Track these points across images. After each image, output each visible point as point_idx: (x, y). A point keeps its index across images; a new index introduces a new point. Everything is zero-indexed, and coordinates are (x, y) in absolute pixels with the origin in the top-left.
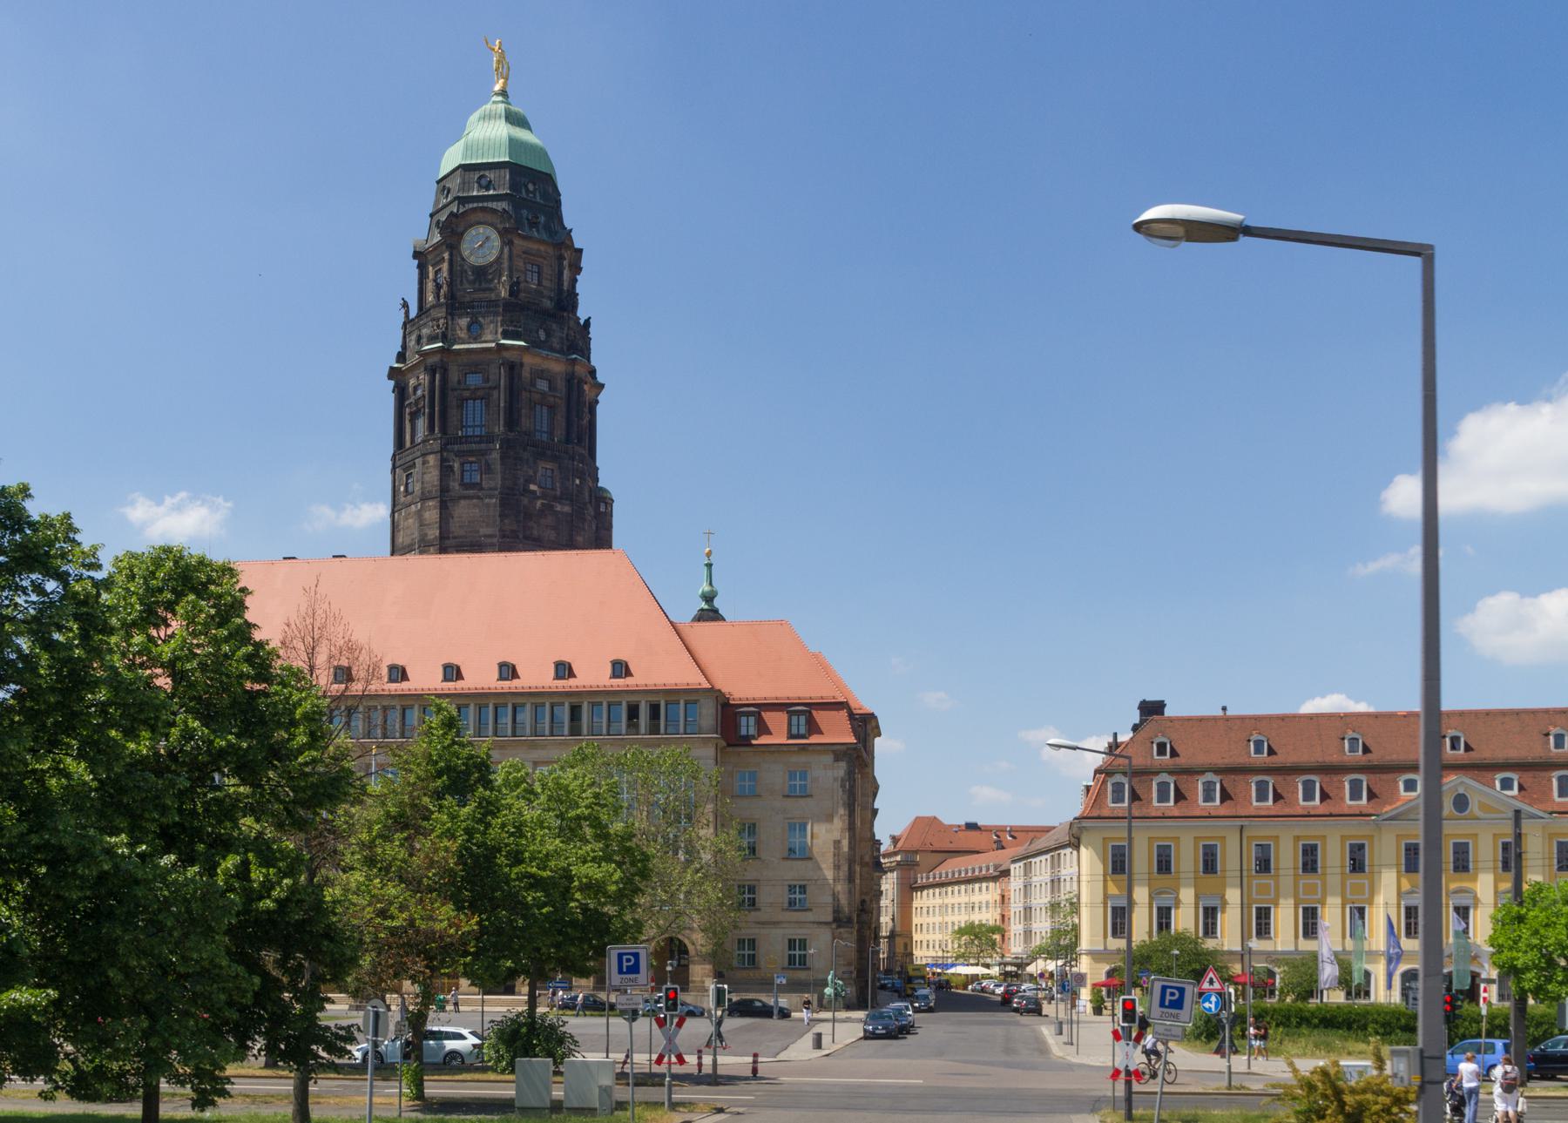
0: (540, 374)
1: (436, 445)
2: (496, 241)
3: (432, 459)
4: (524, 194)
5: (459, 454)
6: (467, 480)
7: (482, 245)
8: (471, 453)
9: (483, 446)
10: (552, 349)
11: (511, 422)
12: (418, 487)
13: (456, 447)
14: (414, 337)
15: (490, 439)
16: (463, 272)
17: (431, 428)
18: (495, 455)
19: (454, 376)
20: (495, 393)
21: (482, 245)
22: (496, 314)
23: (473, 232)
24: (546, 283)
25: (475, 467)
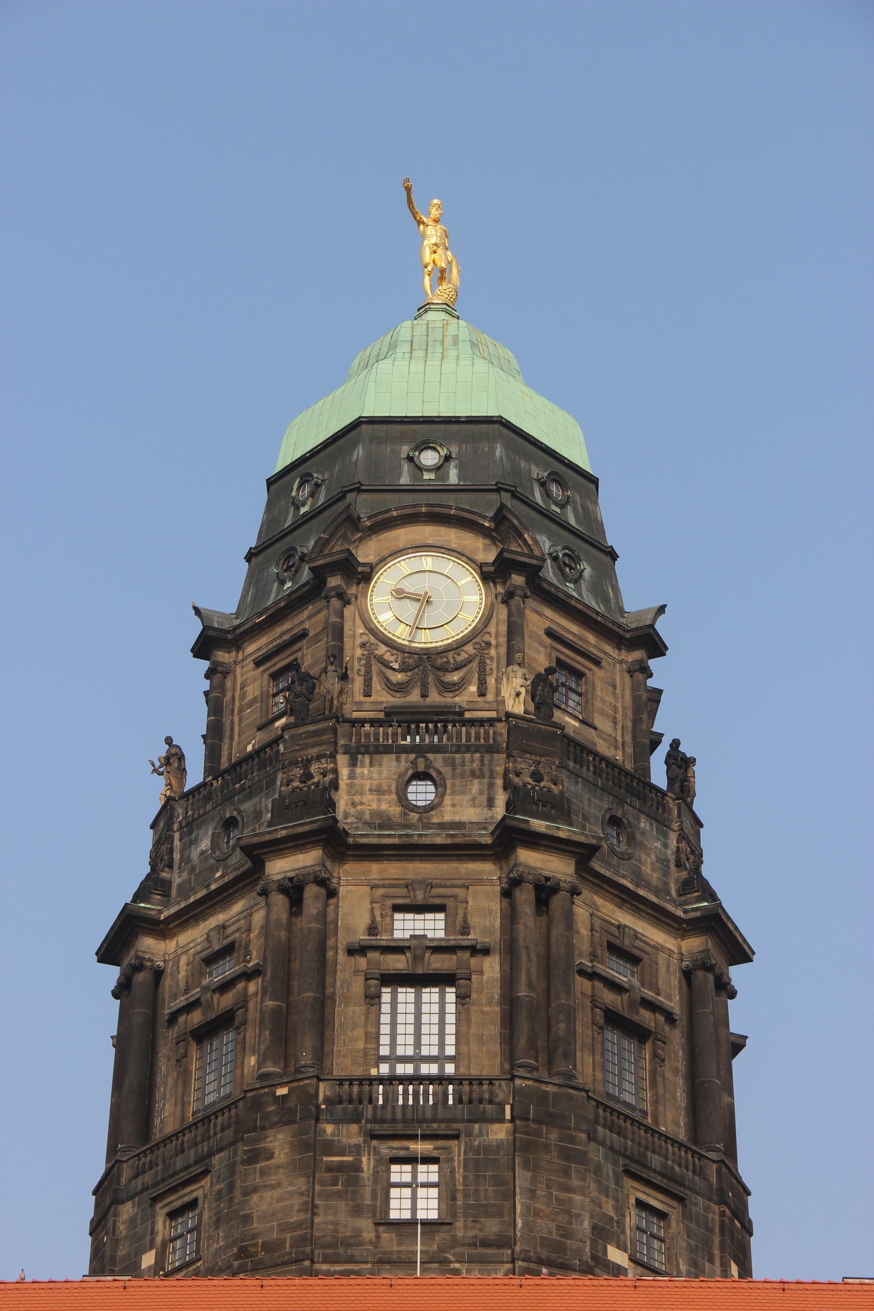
4: (538, 497)
16: (371, 657)
21: (426, 594)
22: (491, 749)
23: (403, 566)
24: (599, 721)
25: (429, 1173)
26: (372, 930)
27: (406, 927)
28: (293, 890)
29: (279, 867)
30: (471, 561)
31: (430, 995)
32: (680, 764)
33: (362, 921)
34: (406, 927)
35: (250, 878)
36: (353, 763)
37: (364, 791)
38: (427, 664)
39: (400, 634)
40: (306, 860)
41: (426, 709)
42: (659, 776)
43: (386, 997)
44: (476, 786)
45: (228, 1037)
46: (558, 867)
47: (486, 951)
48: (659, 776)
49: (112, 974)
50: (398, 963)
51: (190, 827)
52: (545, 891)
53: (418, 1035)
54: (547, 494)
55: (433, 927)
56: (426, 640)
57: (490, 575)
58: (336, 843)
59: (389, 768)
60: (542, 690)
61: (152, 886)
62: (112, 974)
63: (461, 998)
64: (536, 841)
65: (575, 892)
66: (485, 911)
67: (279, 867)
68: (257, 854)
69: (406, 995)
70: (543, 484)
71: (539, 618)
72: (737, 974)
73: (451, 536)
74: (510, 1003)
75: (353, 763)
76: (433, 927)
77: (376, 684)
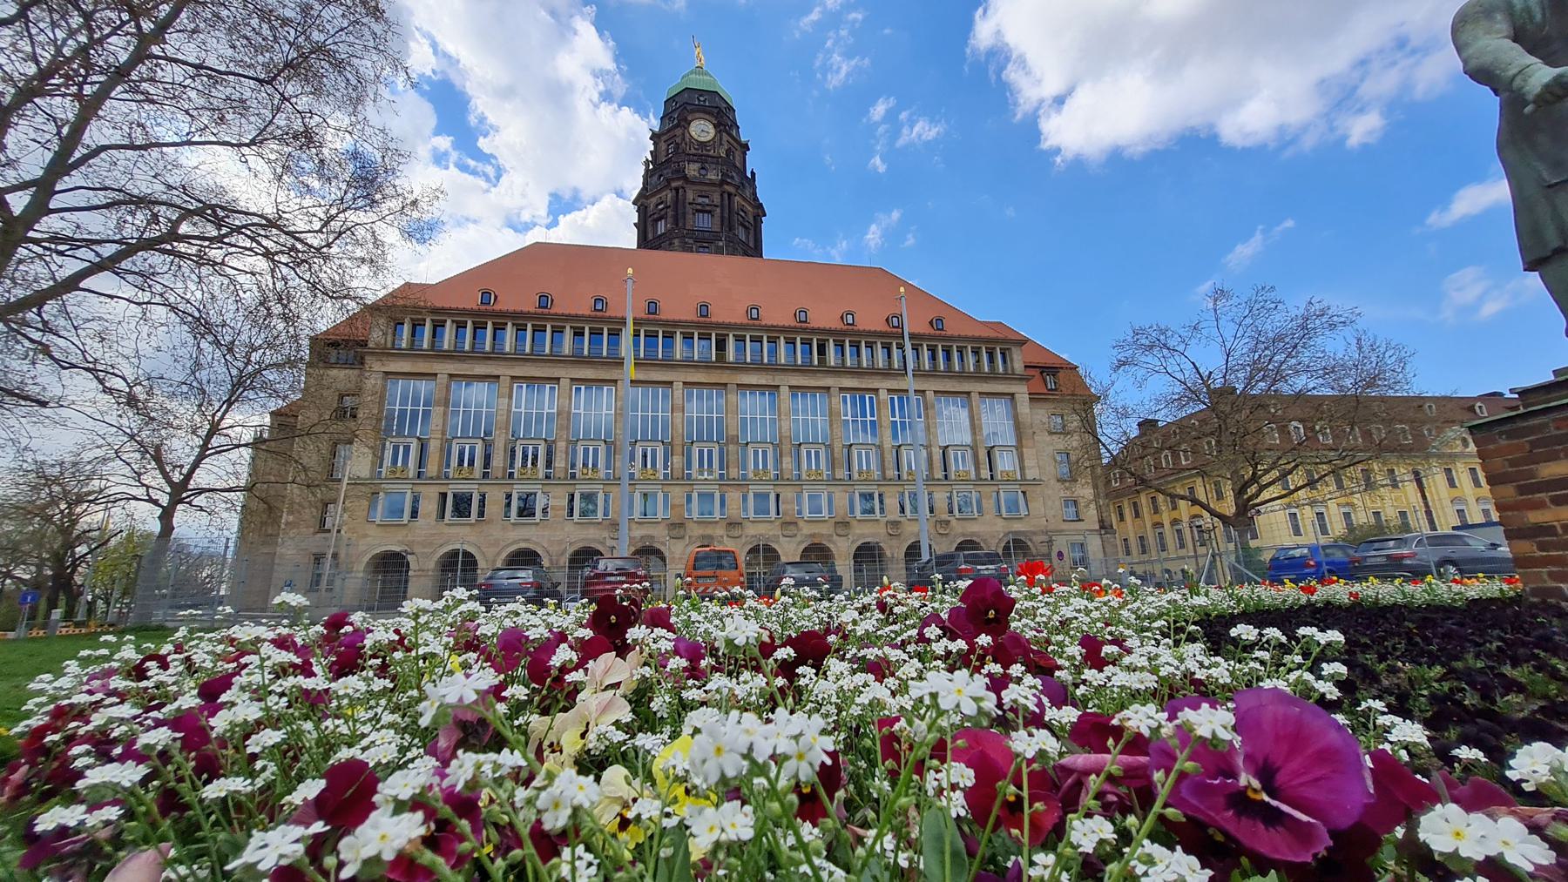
2: (712, 131)
7: (702, 130)
19: (690, 196)
21: (702, 130)
27: (700, 200)
28: (677, 190)
29: (674, 184)
32: (753, 174)
34: (700, 200)
35: (668, 186)
37: (692, 170)
38: (703, 145)
41: (702, 154)
46: (731, 189)
52: (730, 195)
58: (685, 178)
59: (697, 166)
60: (728, 152)
61: (644, 188)
66: (717, 199)
67: (674, 184)
68: (669, 181)
71: (725, 137)
74: (722, 217)
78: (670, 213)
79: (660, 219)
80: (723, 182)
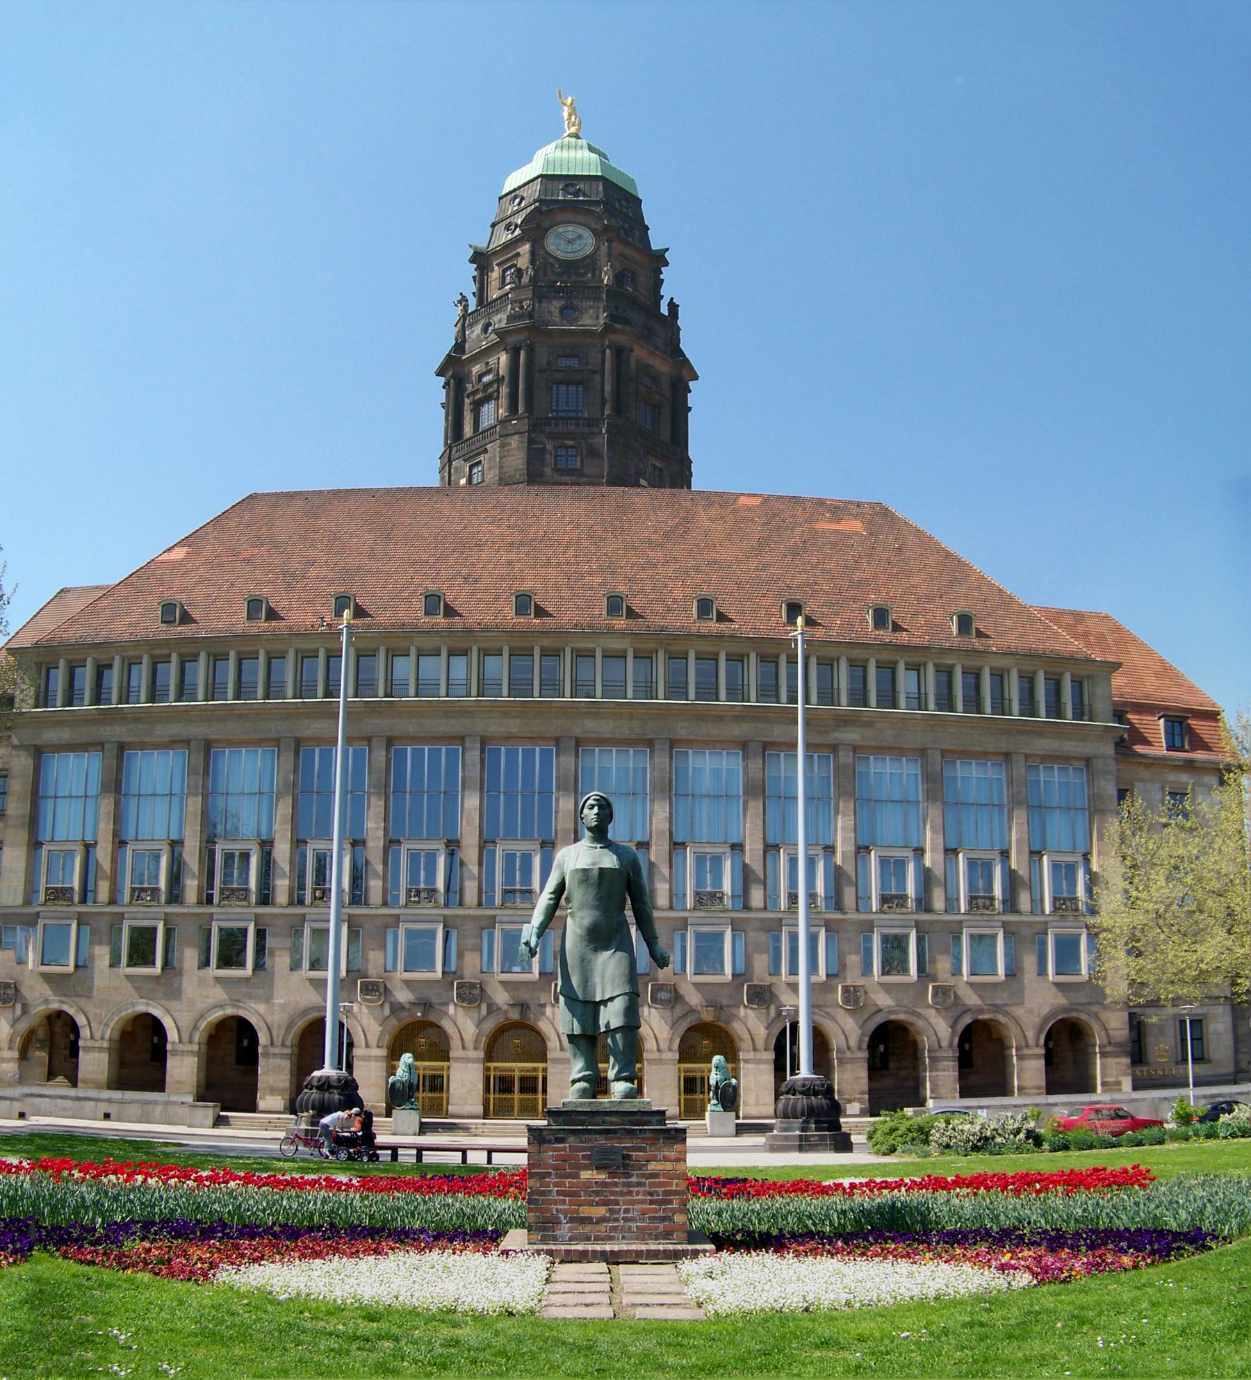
0: (646, 369)
1: (524, 425)
3: (514, 441)
5: (551, 436)
6: (562, 465)
7: (572, 241)
8: (568, 436)
9: (586, 430)
10: (656, 347)
11: (618, 410)
12: (492, 475)
13: (548, 429)
14: (478, 329)
15: (593, 422)
17: (513, 407)
18: (602, 440)
19: (543, 357)
20: (597, 378)
22: (599, 299)
26: (549, 363)
27: (563, 362)
30: (589, 228)
31: (572, 388)
33: (544, 361)
34: (563, 362)
36: (540, 302)
39: (559, 254)
40: (522, 337)
42: (664, 310)
43: (555, 388)
44: (591, 311)
45: (492, 404)
47: (594, 372)
48: (664, 310)
49: (442, 380)
50: (560, 376)
51: (471, 325)
53: (567, 402)
54: (621, 205)
55: (574, 363)
56: (571, 257)
57: (595, 232)
60: (619, 278)
61: (459, 346)
62: (442, 380)
63: (586, 389)
64: (615, 331)
65: (632, 351)
69: (563, 388)
70: (620, 201)
72: (692, 384)
73: (581, 218)
75: (540, 302)
76: (574, 363)
77: (549, 273)
78: (504, 390)
79: (487, 399)
80: (608, 329)
